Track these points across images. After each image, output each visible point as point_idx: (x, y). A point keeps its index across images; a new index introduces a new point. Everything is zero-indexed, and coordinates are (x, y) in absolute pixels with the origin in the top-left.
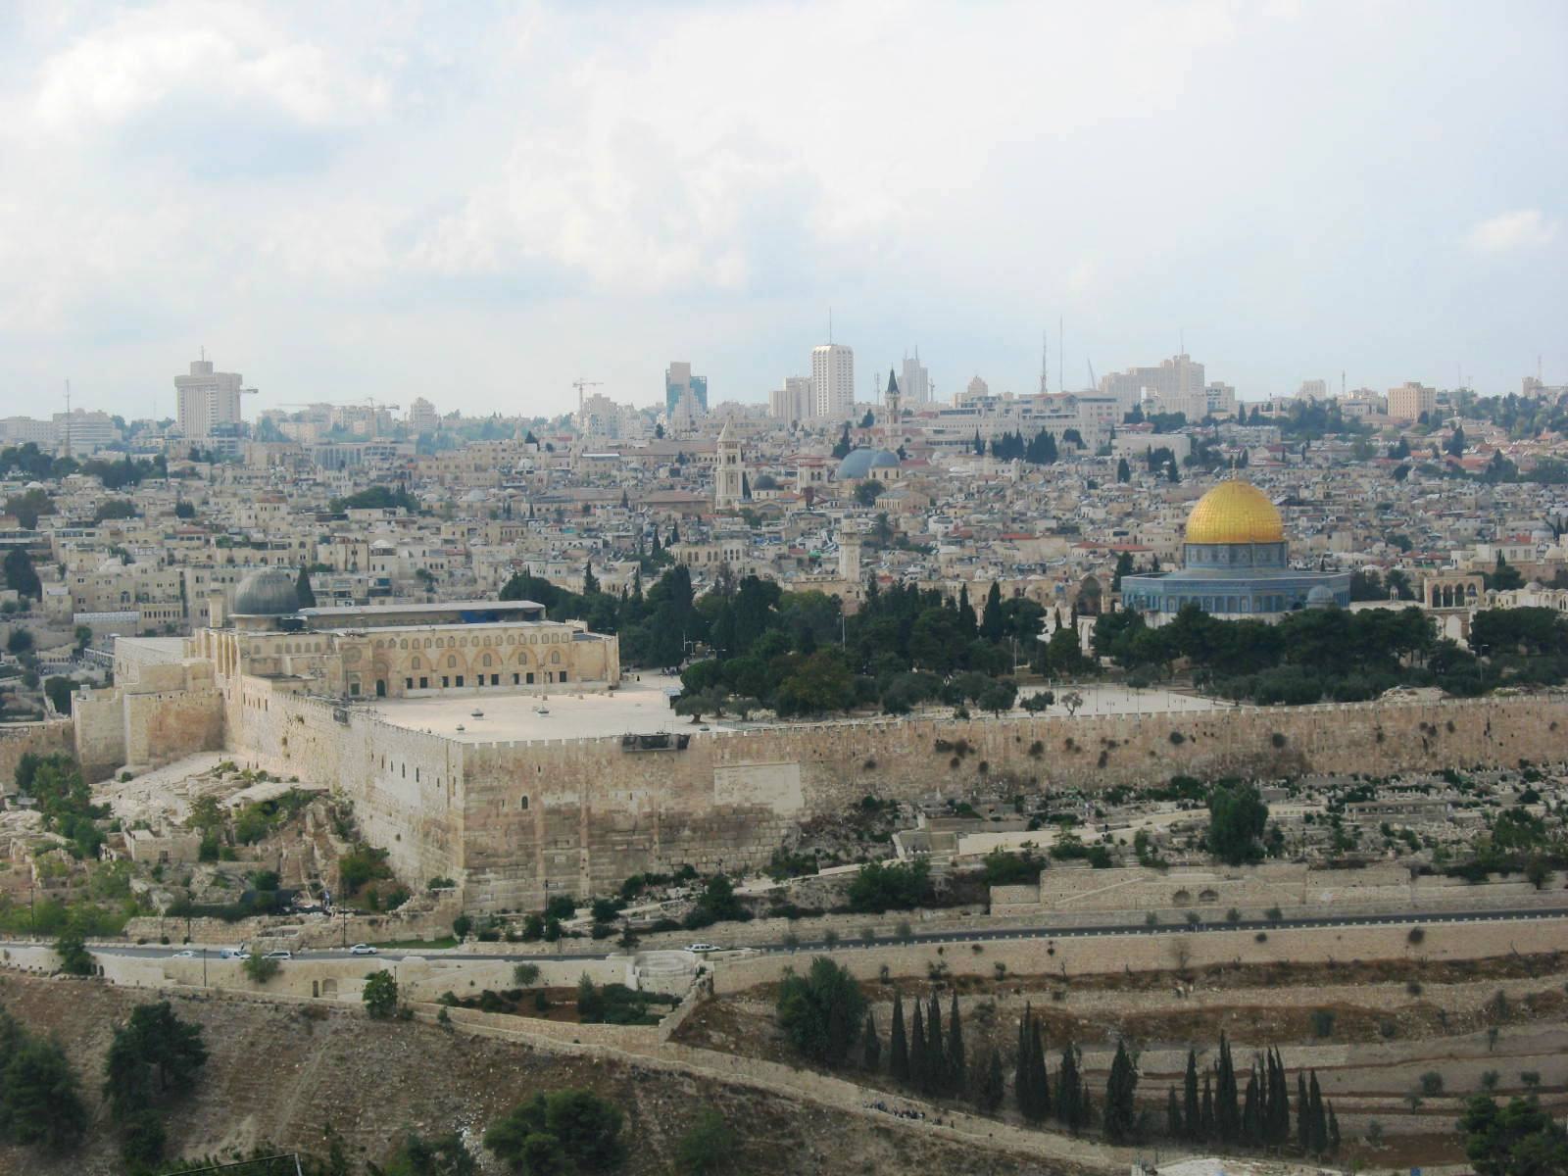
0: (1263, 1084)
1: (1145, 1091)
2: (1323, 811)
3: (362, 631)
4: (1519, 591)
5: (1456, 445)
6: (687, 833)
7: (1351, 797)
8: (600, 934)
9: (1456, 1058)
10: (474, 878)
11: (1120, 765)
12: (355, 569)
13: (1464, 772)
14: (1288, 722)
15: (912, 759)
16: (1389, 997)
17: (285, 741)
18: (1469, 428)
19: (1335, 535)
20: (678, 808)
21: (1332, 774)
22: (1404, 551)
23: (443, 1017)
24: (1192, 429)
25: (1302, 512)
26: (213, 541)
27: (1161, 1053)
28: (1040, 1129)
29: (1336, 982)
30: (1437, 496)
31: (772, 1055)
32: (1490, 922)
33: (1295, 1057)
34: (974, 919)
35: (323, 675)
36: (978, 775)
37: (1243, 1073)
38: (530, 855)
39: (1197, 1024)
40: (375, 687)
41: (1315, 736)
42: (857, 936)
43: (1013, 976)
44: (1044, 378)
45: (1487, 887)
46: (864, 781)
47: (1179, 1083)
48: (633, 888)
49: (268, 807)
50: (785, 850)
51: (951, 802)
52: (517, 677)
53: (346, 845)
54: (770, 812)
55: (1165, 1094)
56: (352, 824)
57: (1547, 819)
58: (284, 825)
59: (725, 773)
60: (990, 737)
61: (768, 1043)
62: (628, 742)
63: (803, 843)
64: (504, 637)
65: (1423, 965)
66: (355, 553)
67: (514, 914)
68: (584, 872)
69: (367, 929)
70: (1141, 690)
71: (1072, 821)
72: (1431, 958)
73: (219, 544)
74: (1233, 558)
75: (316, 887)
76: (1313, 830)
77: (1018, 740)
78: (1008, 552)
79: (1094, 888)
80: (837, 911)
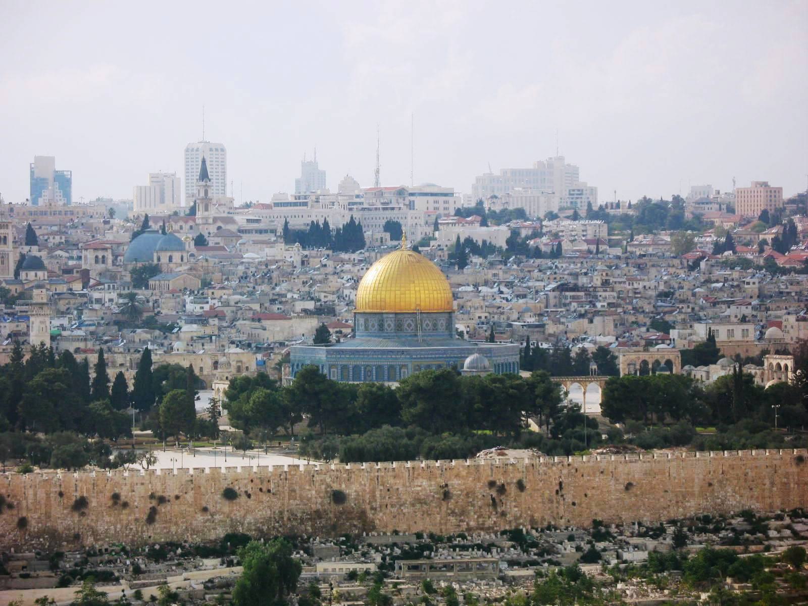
4: (712, 367)
7: (406, 555)
11: (170, 521)
13: (534, 532)
19: (597, 320)
21: (396, 532)
30: (720, 285)
36: (17, 532)
41: (378, 494)
44: (378, 172)
57: (599, 578)
60: (31, 492)
70: (248, 452)
71: (108, 578)
74: (399, 327)
77: (61, 494)
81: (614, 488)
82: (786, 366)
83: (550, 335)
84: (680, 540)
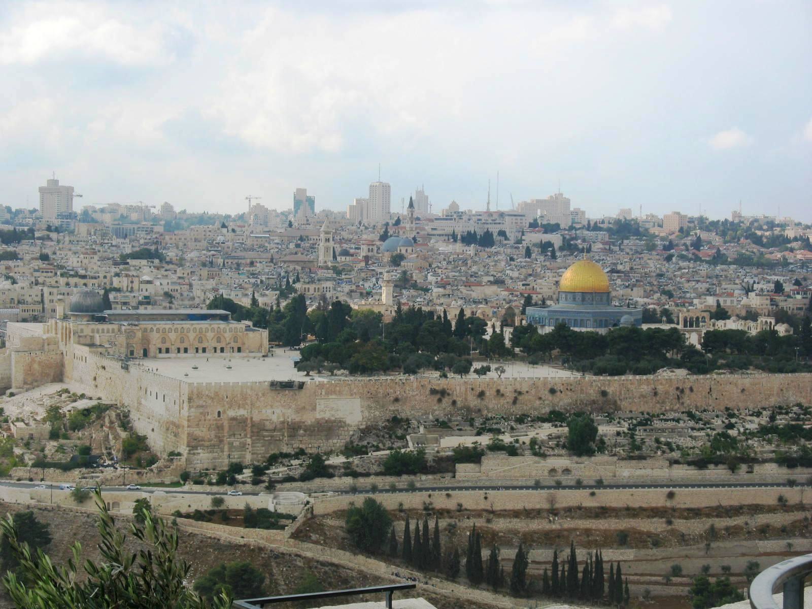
0: (591, 568)
1: (532, 570)
2: (626, 431)
3: (137, 323)
4: (727, 321)
5: (697, 244)
6: (302, 432)
7: (640, 424)
8: (256, 482)
9: (689, 558)
10: (192, 452)
12: (132, 291)
13: (697, 413)
14: (609, 385)
15: (417, 398)
16: (656, 526)
17: (95, 379)
18: (704, 236)
19: (634, 289)
20: (297, 419)
21: (631, 411)
22: (669, 298)
23: (175, 523)
24: (563, 232)
25: (619, 277)
26: (59, 273)
27: (540, 551)
28: (478, 588)
29: (630, 518)
31: (342, 547)
32: (708, 489)
33: (609, 555)
34: (447, 480)
35: (116, 345)
37: (581, 563)
38: (221, 441)
39: (559, 537)
40: (142, 352)
41: (623, 392)
42: (387, 487)
43: (466, 510)
44: (488, 203)
45: (707, 472)
46: (392, 408)
47: (549, 567)
48: (273, 460)
49: (85, 412)
50: (352, 442)
51: (437, 420)
52: (215, 349)
53: (126, 433)
54: (345, 423)
55: (542, 572)
56: (129, 422)
57: (739, 438)
58: (94, 422)
59: (322, 402)
60: (458, 388)
61: (340, 540)
62: (273, 384)
63: (361, 439)
64: (210, 328)
65: (674, 510)
66: (132, 282)
67: (211, 471)
68: (248, 451)
69: (136, 476)
70: (535, 366)
71: (498, 432)
72: (678, 506)
73: (62, 275)
74: (583, 300)
75: (110, 454)
76: (620, 440)
77: (472, 389)
78: (468, 292)
79: (508, 466)
80: (377, 474)
81: (736, 391)
82: (771, 323)
83: (614, 297)
84: (772, 418)
